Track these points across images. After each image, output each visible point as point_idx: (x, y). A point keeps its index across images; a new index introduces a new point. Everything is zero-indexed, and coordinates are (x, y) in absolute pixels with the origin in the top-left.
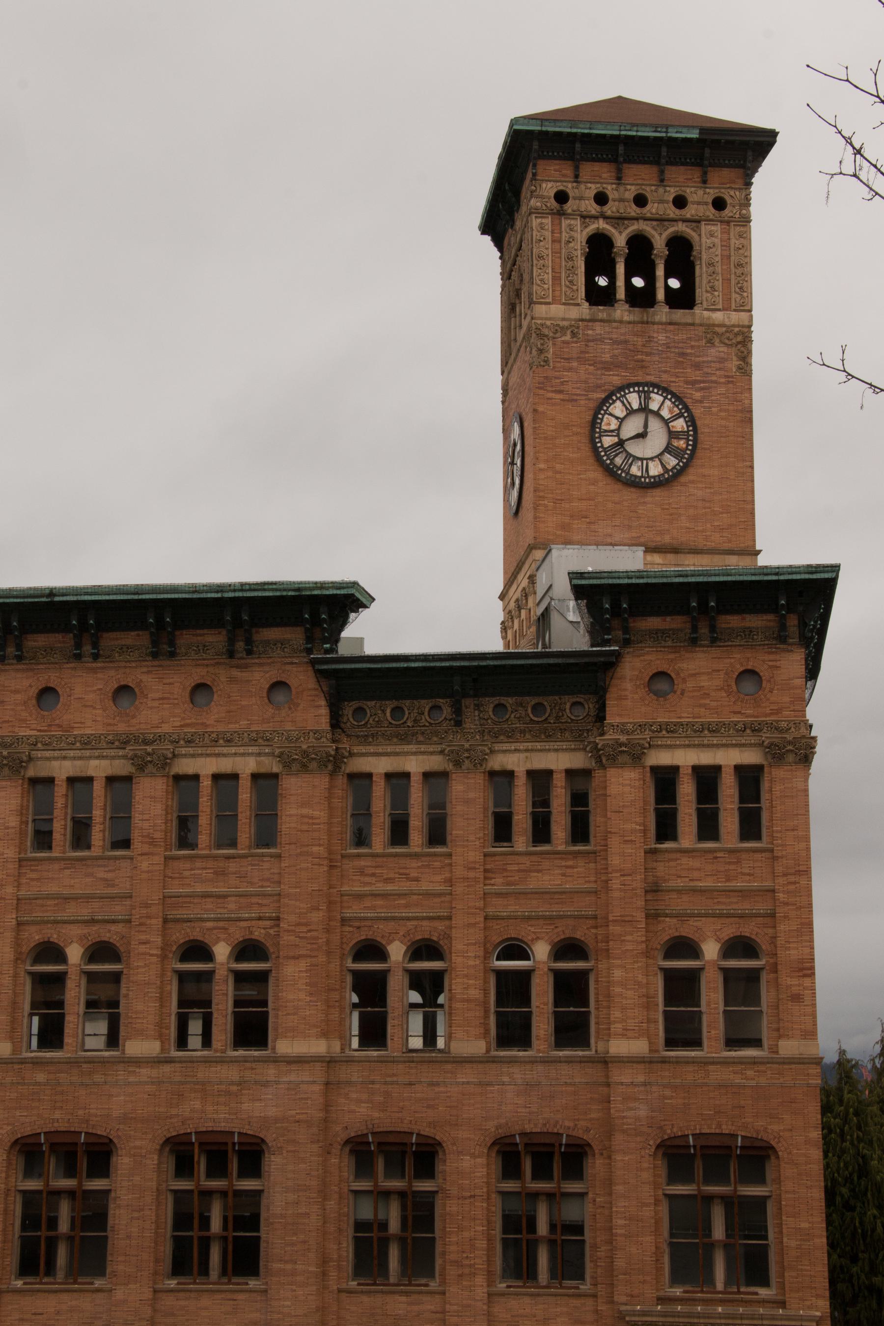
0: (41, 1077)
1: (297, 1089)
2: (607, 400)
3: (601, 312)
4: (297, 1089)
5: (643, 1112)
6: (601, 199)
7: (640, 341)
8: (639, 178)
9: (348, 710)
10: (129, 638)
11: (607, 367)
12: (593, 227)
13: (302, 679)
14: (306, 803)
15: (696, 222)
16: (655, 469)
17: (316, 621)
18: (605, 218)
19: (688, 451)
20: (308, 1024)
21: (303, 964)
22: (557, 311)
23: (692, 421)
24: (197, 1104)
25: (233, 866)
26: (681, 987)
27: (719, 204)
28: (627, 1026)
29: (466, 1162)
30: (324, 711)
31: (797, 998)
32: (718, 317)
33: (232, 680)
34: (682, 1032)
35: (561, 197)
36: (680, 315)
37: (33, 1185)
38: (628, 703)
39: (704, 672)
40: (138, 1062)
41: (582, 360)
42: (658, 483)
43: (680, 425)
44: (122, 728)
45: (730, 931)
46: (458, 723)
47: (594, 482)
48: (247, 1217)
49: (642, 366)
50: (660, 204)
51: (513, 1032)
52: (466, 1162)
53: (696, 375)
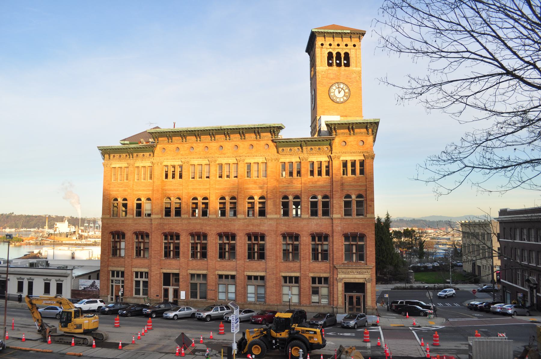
0: (221, 222)
3: (330, 68)
5: (340, 228)
6: (330, 45)
7: (338, 74)
8: (338, 40)
9: (280, 149)
11: (332, 79)
12: (328, 51)
13: (271, 144)
16: (342, 100)
17: (274, 132)
19: (348, 96)
21: (272, 200)
23: (349, 90)
24: (252, 227)
26: (348, 204)
27: (354, 46)
28: (337, 212)
29: (305, 238)
30: (276, 150)
31: (370, 206)
32: (354, 68)
33: (257, 144)
34: (348, 213)
36: (347, 68)
37: (221, 242)
40: (240, 219)
41: (326, 78)
42: (342, 103)
43: (347, 91)
45: (357, 193)
46: (302, 152)
47: (329, 103)
48: (262, 248)
49: (339, 79)
50: (342, 45)
51: (314, 213)
52: (305, 238)
53: (349, 80)
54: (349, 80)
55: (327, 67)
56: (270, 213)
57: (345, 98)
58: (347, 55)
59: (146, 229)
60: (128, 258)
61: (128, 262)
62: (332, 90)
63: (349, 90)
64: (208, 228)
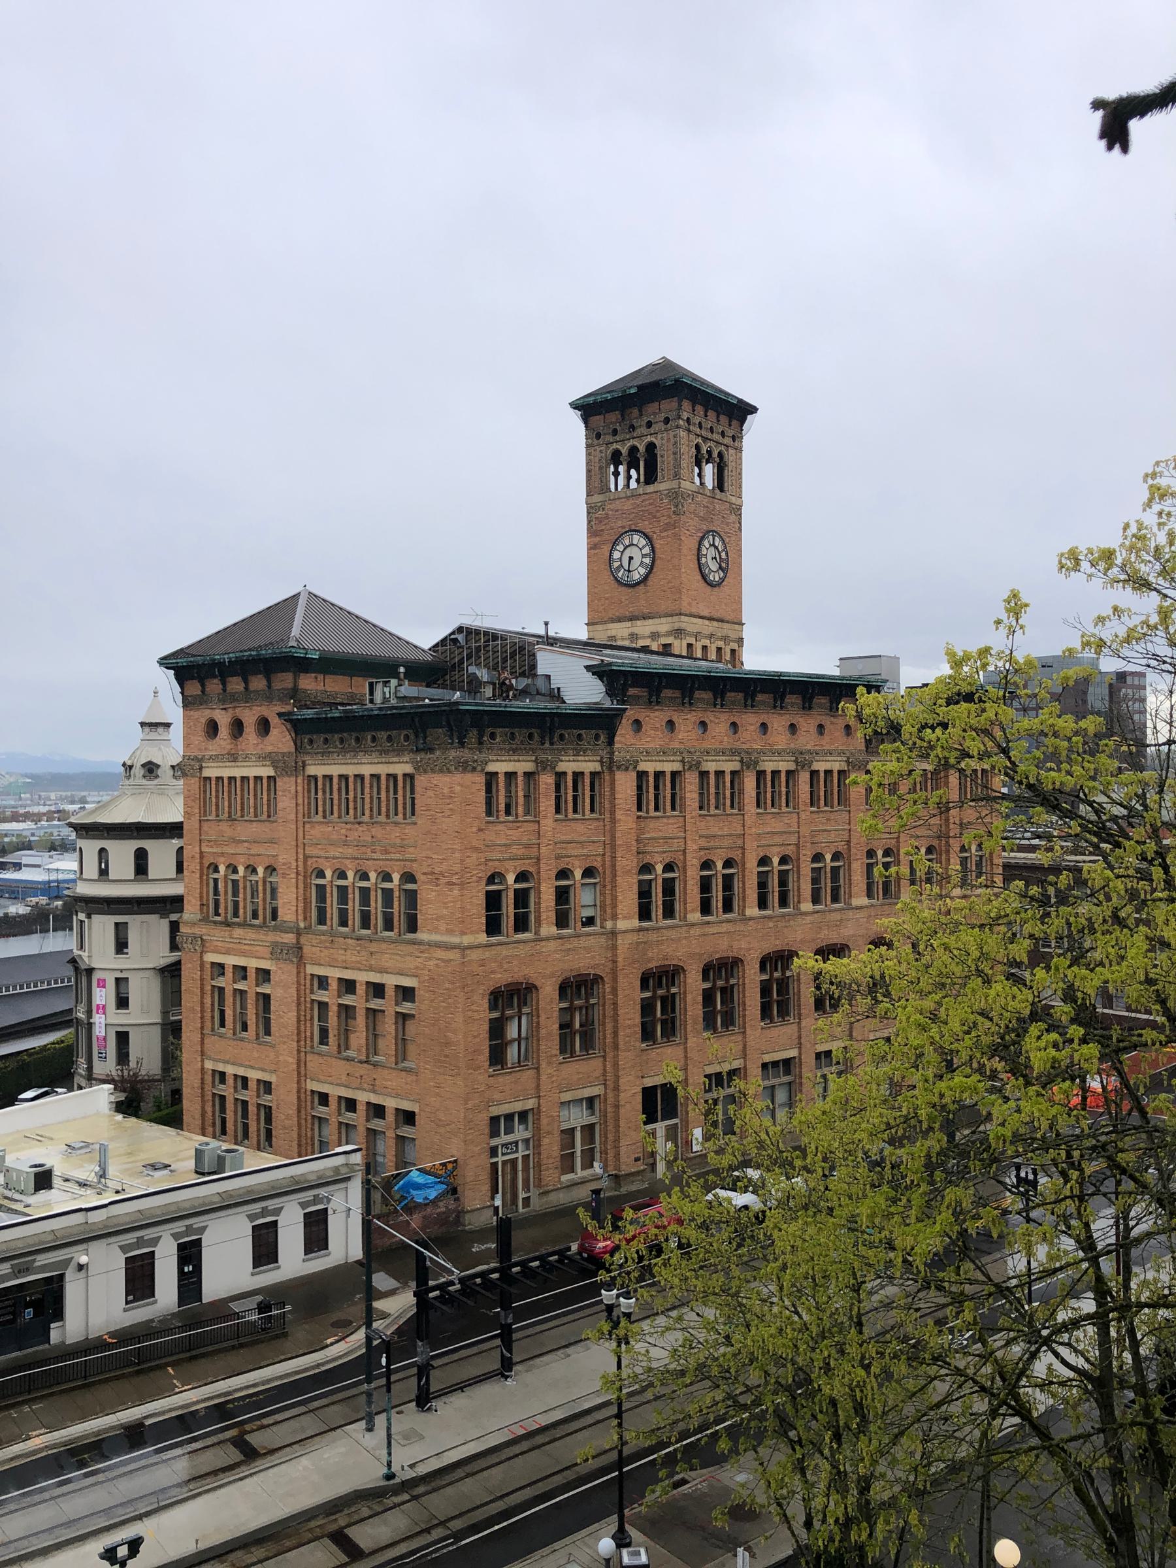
0: (771, 925)
25: (832, 816)
33: (832, 723)
44: (792, 745)
59: (594, 967)
60: (549, 1063)
61: (550, 1076)
64: (744, 945)
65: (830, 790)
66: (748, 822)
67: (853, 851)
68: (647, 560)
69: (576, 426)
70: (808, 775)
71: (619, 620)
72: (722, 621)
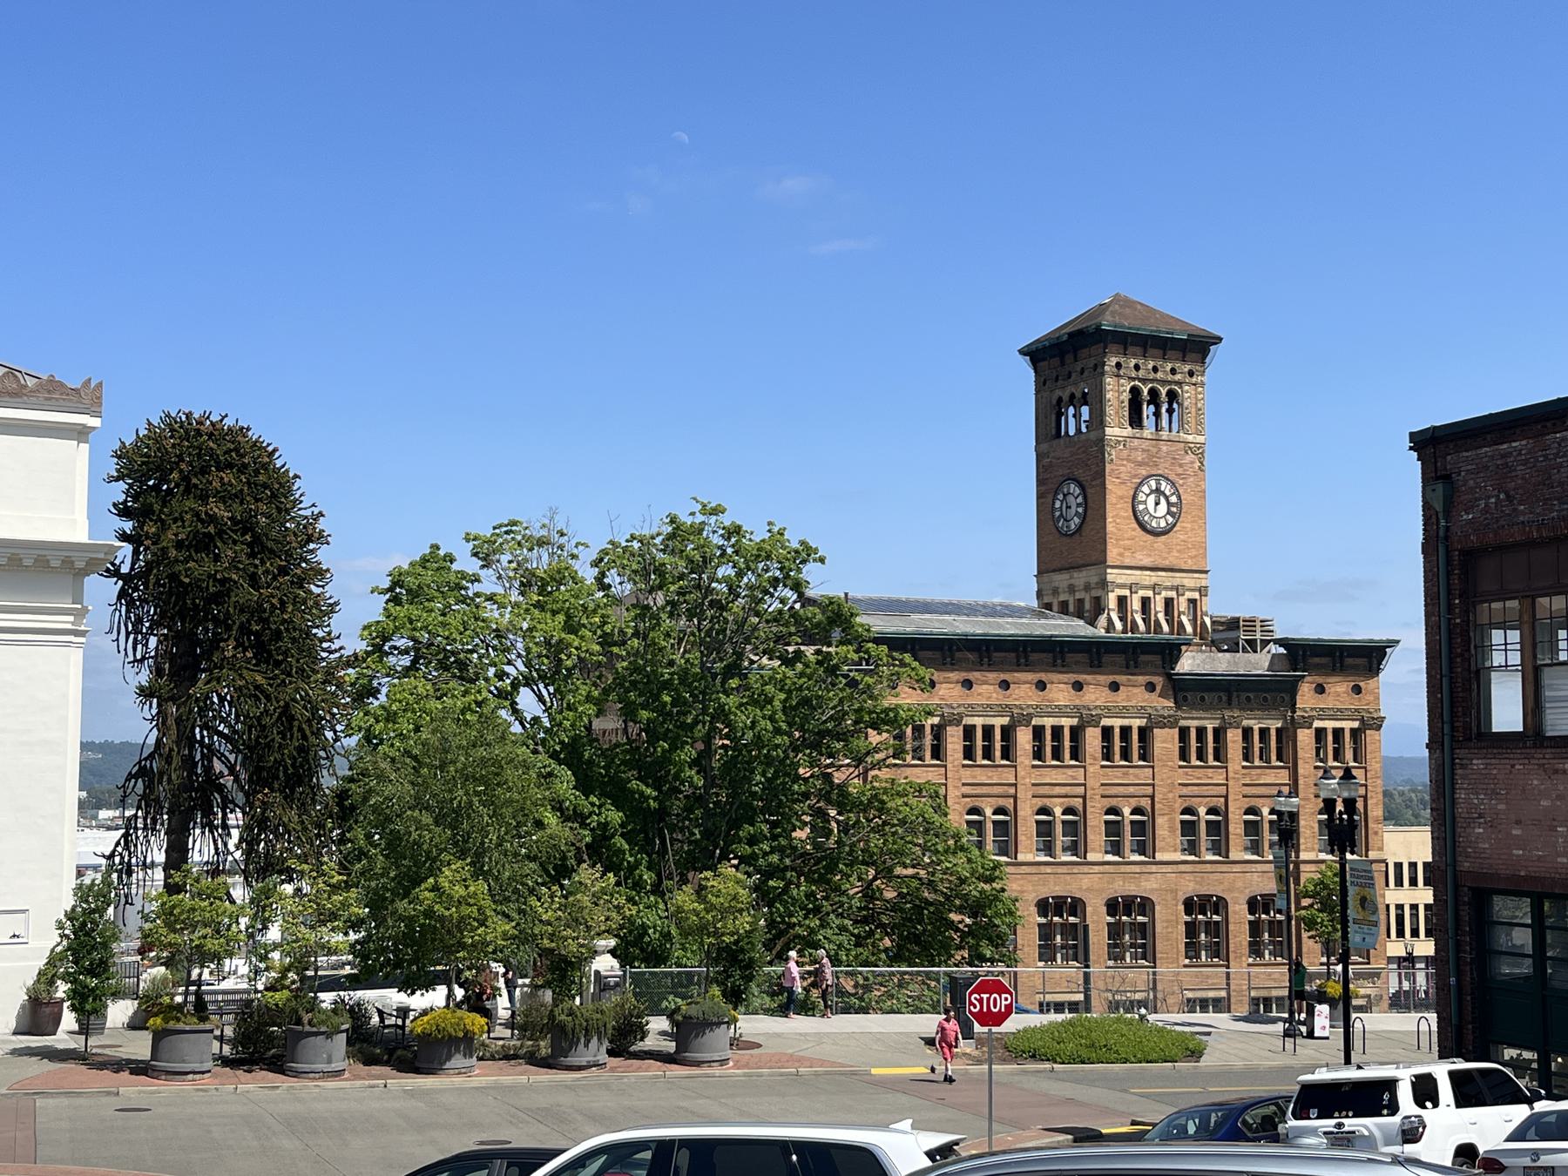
1: (1168, 878)
2: (1141, 484)
4: (1168, 878)
10: (1079, 657)
11: (1140, 464)
13: (1159, 681)
14: (1165, 742)
15: (1179, 383)
16: (1163, 524)
18: (1140, 380)
19: (1176, 511)
20: (1169, 846)
22: (1117, 431)
23: (1179, 497)
32: (1190, 438)
35: (1118, 365)
37: (1043, 920)
38: (1306, 698)
39: (1339, 688)
41: (1128, 460)
43: (1174, 499)
44: (1077, 702)
54: (1180, 471)
55: (1129, 431)
56: (1163, 850)
57: (1170, 519)
58: (1172, 396)
62: (1141, 497)
63: (1179, 497)
65: (1131, 745)
66: (1021, 772)
67: (1157, 806)
68: (1080, 510)
69: (1025, 375)
70: (1098, 731)
71: (1060, 570)
72: (1172, 570)
